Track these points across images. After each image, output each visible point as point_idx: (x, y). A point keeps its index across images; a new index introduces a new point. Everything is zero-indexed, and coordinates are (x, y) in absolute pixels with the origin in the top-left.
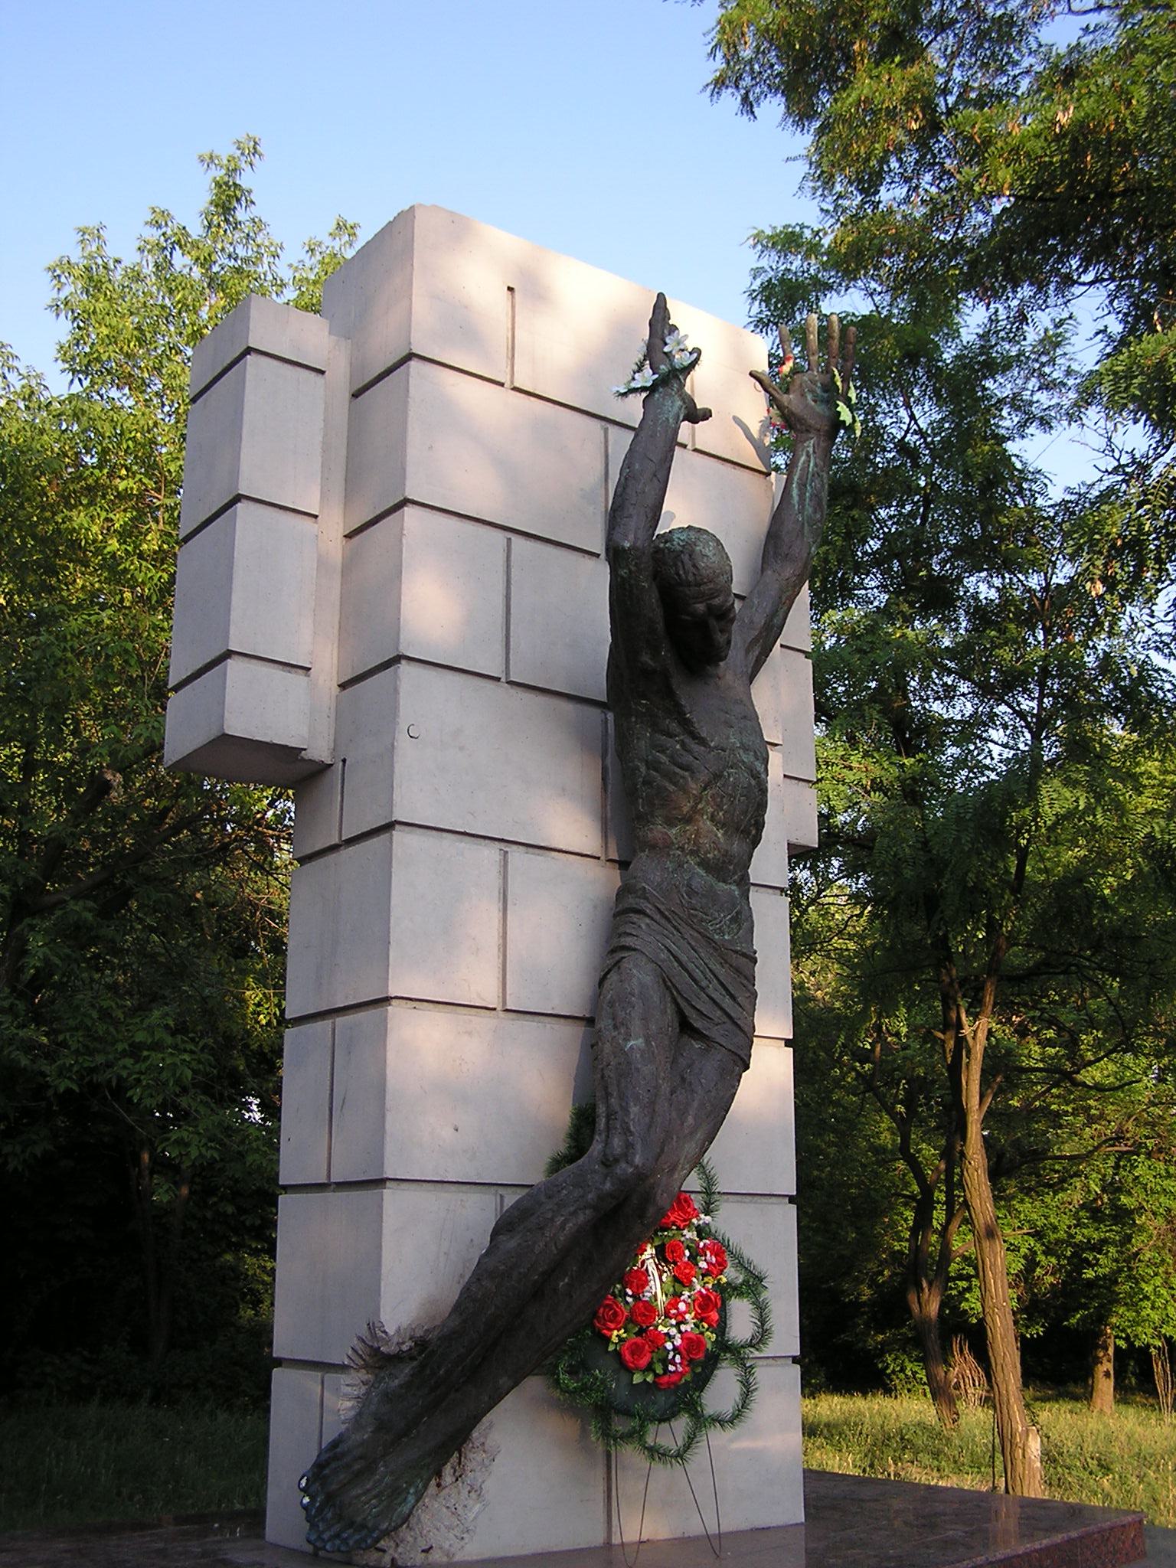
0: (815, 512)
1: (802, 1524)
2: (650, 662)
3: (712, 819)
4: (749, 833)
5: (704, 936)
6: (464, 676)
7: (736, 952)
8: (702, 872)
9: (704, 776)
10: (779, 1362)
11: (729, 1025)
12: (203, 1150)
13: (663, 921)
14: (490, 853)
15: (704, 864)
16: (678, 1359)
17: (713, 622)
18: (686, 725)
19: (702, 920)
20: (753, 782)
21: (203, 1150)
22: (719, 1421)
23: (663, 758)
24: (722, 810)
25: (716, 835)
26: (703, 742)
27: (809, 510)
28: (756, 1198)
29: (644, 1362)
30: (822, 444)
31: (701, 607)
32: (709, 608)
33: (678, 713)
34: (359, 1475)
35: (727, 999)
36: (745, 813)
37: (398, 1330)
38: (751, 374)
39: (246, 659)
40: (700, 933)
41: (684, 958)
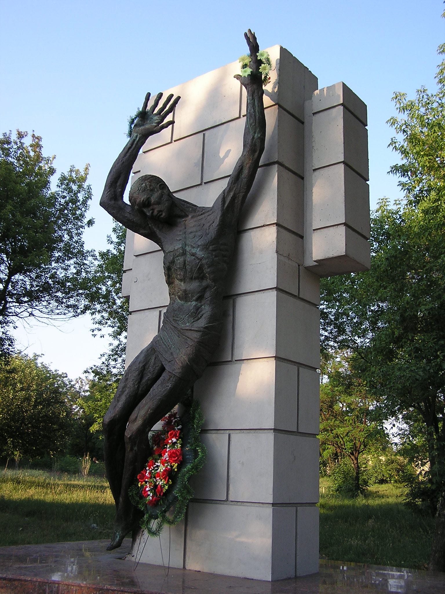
1: (269, 581)
2: (145, 231)
4: (206, 277)
5: (174, 327)
6: (151, 254)
7: (187, 330)
8: (179, 301)
10: (265, 505)
17: (145, 210)
19: (176, 320)
24: (178, 275)
25: (180, 285)
28: (257, 431)
30: (250, 89)
32: (138, 205)
39: (129, 271)
40: (173, 326)
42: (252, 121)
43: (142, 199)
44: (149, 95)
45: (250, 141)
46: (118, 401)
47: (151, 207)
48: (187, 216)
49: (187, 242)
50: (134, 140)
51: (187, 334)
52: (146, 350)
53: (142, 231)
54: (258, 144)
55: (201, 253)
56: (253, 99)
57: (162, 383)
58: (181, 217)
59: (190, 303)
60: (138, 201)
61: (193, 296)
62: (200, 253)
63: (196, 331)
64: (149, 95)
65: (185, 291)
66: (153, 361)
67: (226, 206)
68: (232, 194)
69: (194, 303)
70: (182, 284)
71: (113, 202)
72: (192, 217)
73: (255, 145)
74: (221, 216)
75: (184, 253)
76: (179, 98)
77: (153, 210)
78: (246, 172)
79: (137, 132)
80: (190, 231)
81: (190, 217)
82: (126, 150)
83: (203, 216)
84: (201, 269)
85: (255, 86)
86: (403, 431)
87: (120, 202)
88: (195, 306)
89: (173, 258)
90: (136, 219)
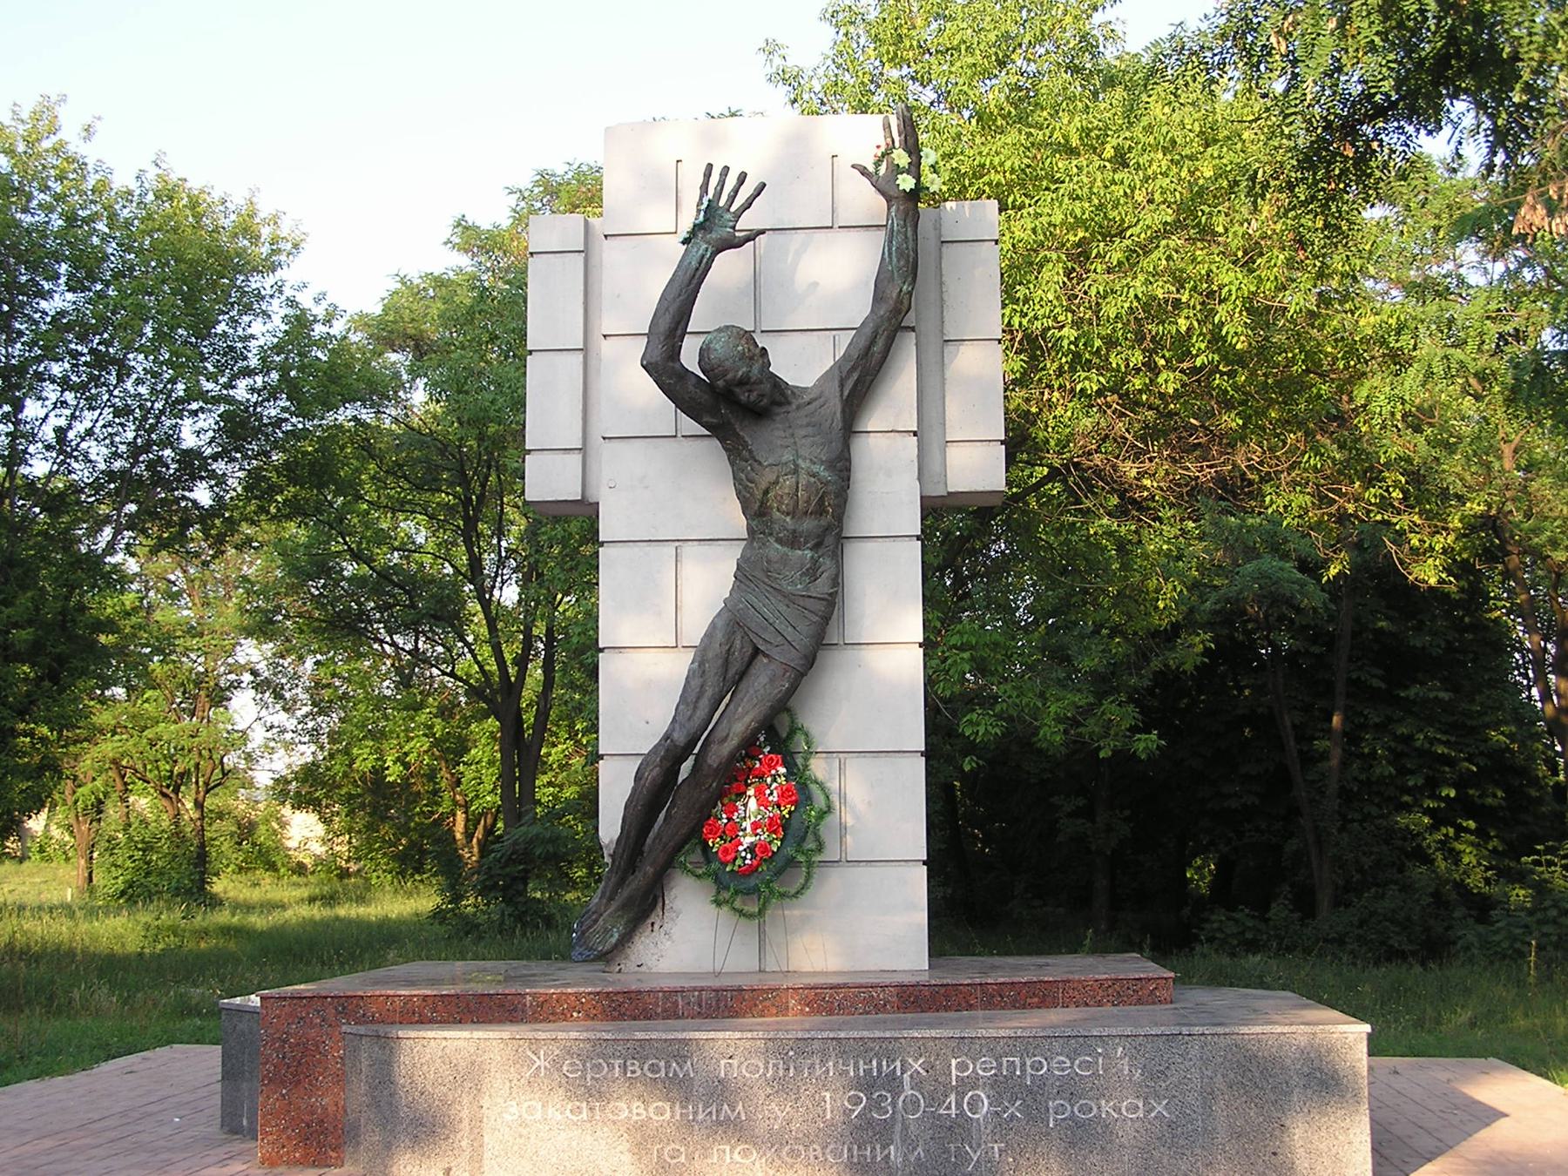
0: (898, 261)
3: (778, 510)
8: (779, 547)
9: (763, 486)
11: (787, 647)
12: (990, 728)
13: (748, 583)
14: (669, 550)
15: (779, 541)
16: (749, 856)
17: (737, 390)
18: (751, 452)
20: (812, 480)
21: (990, 728)
22: (783, 895)
23: (743, 476)
26: (760, 463)
27: (895, 259)
29: (729, 858)
31: (720, 383)
33: (745, 445)
34: (596, 921)
35: (790, 629)
36: (808, 502)
37: (611, 842)
38: (853, 166)
41: (758, 605)
42: (902, 263)
43: (740, 373)
44: (710, 166)
45: (894, 295)
46: (695, 708)
47: (748, 387)
48: (789, 403)
49: (801, 452)
50: (703, 256)
51: (801, 603)
52: (720, 624)
53: (706, 419)
54: (906, 302)
55: (826, 474)
56: (905, 225)
57: (772, 681)
58: (780, 404)
59: (800, 552)
60: (729, 376)
61: (806, 543)
62: (825, 474)
63: (820, 599)
64: (710, 166)
65: (794, 531)
66: (738, 643)
67: (846, 393)
68: (855, 376)
69: (809, 554)
70: (788, 519)
71: (671, 364)
72: (798, 408)
73: (902, 303)
74: (843, 411)
75: (796, 471)
76: (764, 185)
77: (750, 391)
78: (880, 343)
79: (708, 243)
80: (803, 432)
81: (794, 407)
82: (690, 273)
83: (812, 407)
84: (822, 499)
85: (910, 205)
86: (275, 730)
87: (677, 366)
88: (812, 557)
89: (778, 477)
90: (705, 398)
